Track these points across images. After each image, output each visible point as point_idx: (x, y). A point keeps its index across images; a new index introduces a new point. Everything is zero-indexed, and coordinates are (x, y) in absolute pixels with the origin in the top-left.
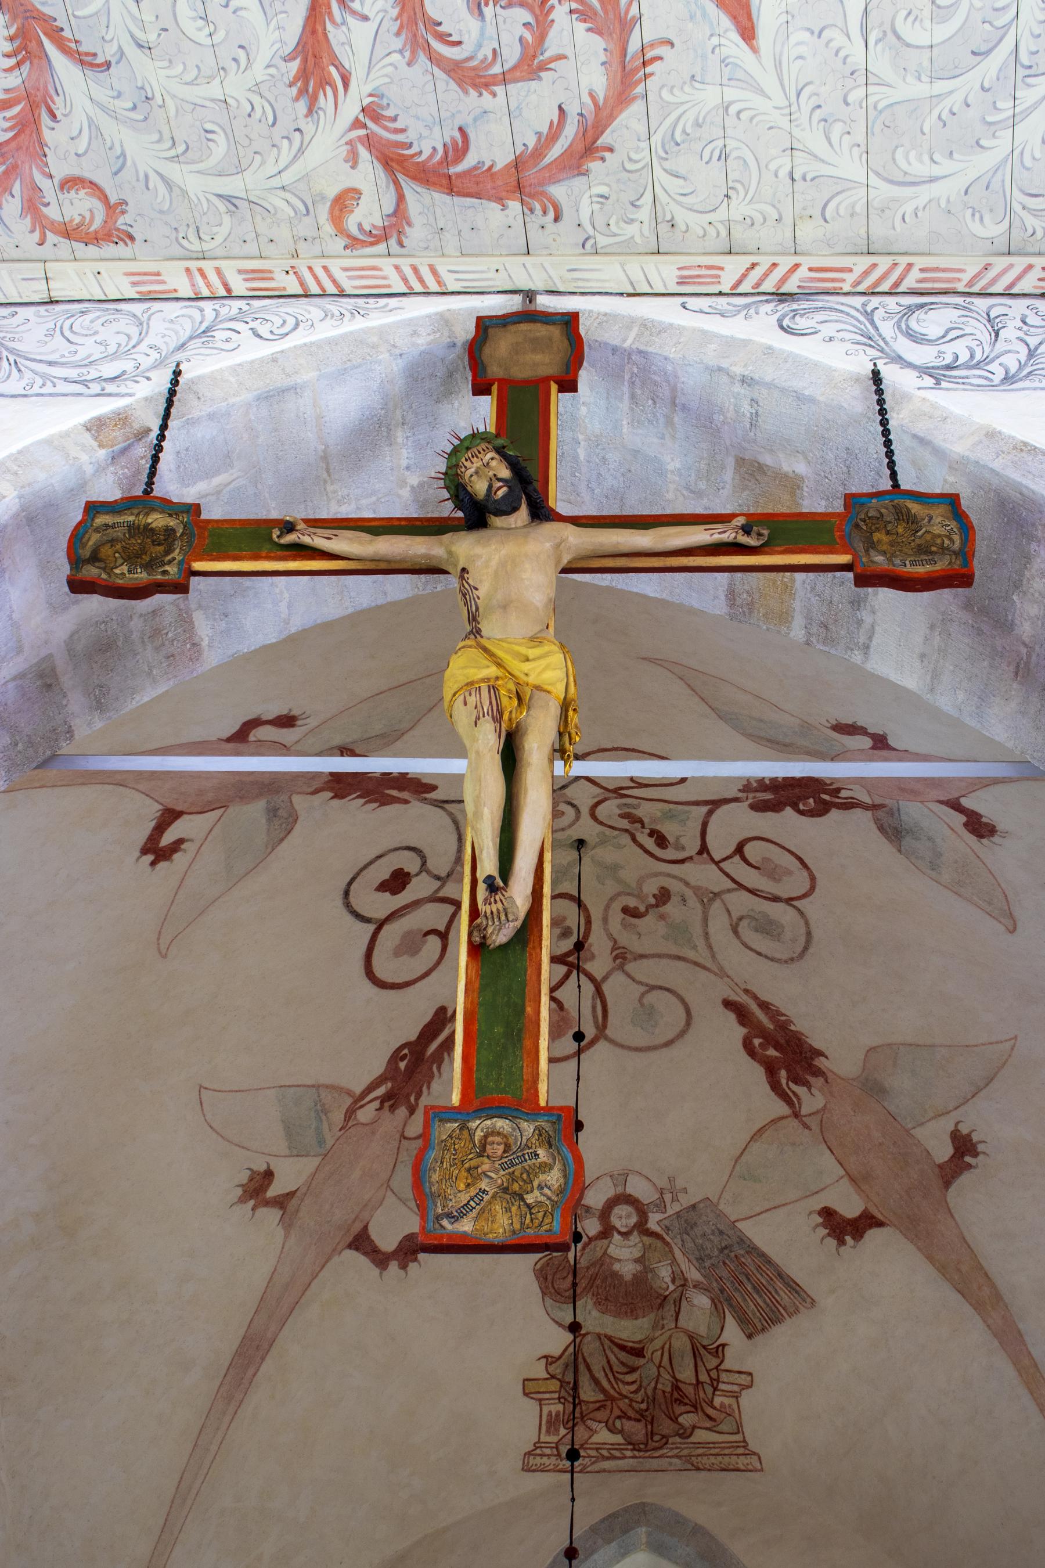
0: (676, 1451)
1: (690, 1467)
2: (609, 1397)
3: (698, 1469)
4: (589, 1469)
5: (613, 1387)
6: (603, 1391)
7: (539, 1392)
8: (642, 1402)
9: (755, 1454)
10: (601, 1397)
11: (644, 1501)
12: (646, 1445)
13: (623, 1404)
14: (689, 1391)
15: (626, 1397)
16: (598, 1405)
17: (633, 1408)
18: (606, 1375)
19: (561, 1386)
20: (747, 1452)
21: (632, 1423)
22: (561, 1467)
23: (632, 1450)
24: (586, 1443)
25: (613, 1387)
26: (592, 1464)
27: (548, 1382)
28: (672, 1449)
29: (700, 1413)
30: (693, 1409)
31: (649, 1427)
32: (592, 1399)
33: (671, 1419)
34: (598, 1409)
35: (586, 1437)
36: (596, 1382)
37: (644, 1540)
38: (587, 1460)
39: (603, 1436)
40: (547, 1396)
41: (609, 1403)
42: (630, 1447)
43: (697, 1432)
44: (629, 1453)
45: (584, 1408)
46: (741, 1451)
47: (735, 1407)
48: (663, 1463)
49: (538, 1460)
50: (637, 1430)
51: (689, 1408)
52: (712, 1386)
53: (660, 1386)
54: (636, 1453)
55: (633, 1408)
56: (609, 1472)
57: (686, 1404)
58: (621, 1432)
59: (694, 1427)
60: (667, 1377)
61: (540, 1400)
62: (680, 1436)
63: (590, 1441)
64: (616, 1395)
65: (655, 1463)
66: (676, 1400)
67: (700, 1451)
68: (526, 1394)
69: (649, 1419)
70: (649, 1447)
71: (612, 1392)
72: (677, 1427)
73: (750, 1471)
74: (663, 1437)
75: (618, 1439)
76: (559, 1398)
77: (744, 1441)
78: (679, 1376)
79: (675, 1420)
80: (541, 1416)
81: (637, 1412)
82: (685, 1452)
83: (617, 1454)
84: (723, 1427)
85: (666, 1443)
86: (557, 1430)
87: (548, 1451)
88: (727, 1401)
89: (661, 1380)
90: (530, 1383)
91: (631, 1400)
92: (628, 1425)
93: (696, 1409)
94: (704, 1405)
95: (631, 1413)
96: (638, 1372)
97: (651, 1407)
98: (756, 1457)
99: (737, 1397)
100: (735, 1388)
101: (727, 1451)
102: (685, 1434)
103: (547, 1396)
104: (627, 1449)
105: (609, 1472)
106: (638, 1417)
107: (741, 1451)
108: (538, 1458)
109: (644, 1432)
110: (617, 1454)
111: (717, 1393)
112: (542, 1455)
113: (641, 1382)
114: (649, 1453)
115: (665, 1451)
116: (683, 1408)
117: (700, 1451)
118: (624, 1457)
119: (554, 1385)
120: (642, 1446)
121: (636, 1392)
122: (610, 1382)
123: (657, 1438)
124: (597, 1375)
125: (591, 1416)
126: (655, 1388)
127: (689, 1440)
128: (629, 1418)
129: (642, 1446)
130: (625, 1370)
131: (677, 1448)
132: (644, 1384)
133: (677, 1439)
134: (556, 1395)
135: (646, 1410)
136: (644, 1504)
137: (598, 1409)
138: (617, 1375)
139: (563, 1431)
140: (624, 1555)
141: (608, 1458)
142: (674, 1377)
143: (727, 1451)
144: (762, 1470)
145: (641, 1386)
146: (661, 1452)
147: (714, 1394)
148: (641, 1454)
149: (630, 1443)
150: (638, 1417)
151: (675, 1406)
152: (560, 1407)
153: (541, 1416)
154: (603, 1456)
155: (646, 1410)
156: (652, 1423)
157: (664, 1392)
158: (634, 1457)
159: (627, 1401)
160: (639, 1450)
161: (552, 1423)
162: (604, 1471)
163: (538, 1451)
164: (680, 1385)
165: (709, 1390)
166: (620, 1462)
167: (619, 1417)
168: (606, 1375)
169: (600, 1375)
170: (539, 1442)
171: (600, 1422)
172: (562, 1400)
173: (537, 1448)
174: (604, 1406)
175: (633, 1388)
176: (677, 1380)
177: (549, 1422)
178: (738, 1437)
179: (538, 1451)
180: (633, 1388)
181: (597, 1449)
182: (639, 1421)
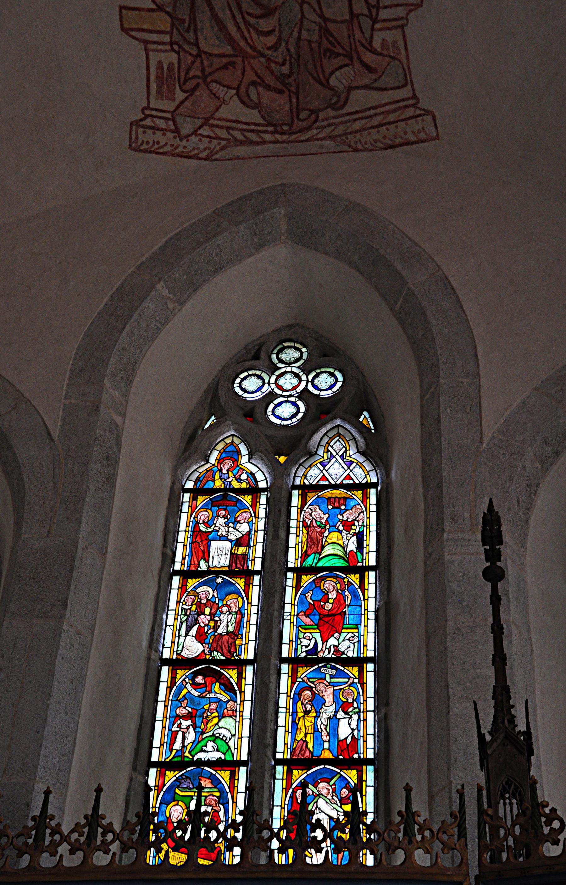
0: (328, 130)
1: (346, 148)
2: (238, 51)
3: (356, 150)
4: (217, 156)
5: (243, 37)
6: (231, 41)
7: (143, 30)
8: (283, 64)
9: (428, 112)
10: (229, 50)
11: (285, 182)
12: (291, 125)
13: (259, 63)
14: (340, 32)
15: (263, 55)
16: (225, 60)
17: (272, 72)
18: (234, 16)
19: (173, 25)
20: (418, 112)
21: (273, 94)
22: (180, 149)
23: (273, 133)
24: (212, 117)
25: (243, 37)
26: (221, 149)
27: (154, 15)
28: (324, 127)
29: (357, 63)
30: (347, 61)
31: (294, 100)
32: (216, 51)
33: (321, 83)
34: (225, 67)
35: (212, 108)
36: (222, 27)
37: (284, 228)
38: (215, 142)
39: (233, 110)
40: (154, 37)
41: (239, 60)
42: (270, 129)
43: (355, 95)
44: (268, 137)
45: (206, 63)
46: (410, 112)
47: (401, 44)
48: (313, 146)
49: (150, 136)
50: (279, 104)
51: (342, 60)
52: (370, 17)
53: (305, 34)
54: (279, 137)
55: (272, 72)
56: (244, 159)
57: (339, 55)
58: (257, 106)
59: (350, 89)
60: (313, 17)
61: (146, 42)
62: (333, 107)
63: (217, 115)
64: (249, 50)
65: (302, 148)
66: (327, 50)
67: (358, 125)
68: (125, 30)
69: (293, 89)
70: (294, 129)
71: (242, 43)
72: (329, 93)
73: (423, 141)
74: (312, 111)
75: (254, 116)
76: (171, 43)
77: (415, 97)
78: (328, 13)
79: (326, 85)
80: (148, 68)
81: (277, 78)
82: (340, 130)
83: (254, 137)
84: (387, 80)
85: (316, 121)
86: (172, 92)
87: (161, 124)
88: (389, 36)
89: (305, 23)
90: (130, 13)
91: (269, 60)
92: (267, 97)
93: (351, 59)
94: (361, 49)
95: (270, 80)
96: (276, 16)
97: (295, 70)
98: (429, 118)
99: (402, 27)
100: (400, 12)
101: (391, 118)
102: (338, 102)
103: (154, 37)
104: (266, 132)
105: (244, 159)
106: (279, 86)
107: (410, 112)
108: (149, 132)
109: (287, 108)
110: (254, 137)
111: (377, 26)
112: (155, 129)
113: (281, 32)
114: (293, 137)
115: (315, 131)
116: (336, 62)
117: (358, 125)
118: (264, 142)
119: (163, 22)
120: (285, 128)
121: (274, 47)
122: (239, 28)
123: (304, 115)
124: (221, 15)
125: (217, 76)
126: (299, 39)
127: (344, 111)
128: (268, 87)
129: (285, 128)
130: (258, 12)
131: (329, 125)
132: (285, 35)
133: (330, 112)
134: (167, 38)
135: (289, 76)
136: (284, 185)
137: (225, 67)
138: (248, 18)
139: (180, 96)
140: (259, 247)
141: (242, 143)
142: (322, 16)
143: (391, 118)
144: (437, 138)
145: (280, 39)
146: (309, 134)
147: (373, 29)
148: (285, 137)
149: (270, 124)
150: (279, 86)
151: (325, 61)
152: (173, 58)
153: (148, 68)
154: (236, 140)
155: (289, 76)
156: (297, 94)
157: (310, 42)
158: (276, 142)
159: (263, 60)
160: (282, 133)
161: (164, 81)
162: (238, 158)
163: (148, 122)
164: (330, 26)
165: (366, 23)
166: (259, 148)
167: (253, 83)
168: (234, 16)
169: (225, 16)
170: (148, 108)
171: (229, 87)
172: (176, 47)
173: (147, 116)
174: (233, 64)
175: (271, 40)
176: (326, 20)
177: (159, 77)
178: (406, 92)
179: (148, 122)
180: (271, 40)
181: (228, 129)
182: (280, 92)
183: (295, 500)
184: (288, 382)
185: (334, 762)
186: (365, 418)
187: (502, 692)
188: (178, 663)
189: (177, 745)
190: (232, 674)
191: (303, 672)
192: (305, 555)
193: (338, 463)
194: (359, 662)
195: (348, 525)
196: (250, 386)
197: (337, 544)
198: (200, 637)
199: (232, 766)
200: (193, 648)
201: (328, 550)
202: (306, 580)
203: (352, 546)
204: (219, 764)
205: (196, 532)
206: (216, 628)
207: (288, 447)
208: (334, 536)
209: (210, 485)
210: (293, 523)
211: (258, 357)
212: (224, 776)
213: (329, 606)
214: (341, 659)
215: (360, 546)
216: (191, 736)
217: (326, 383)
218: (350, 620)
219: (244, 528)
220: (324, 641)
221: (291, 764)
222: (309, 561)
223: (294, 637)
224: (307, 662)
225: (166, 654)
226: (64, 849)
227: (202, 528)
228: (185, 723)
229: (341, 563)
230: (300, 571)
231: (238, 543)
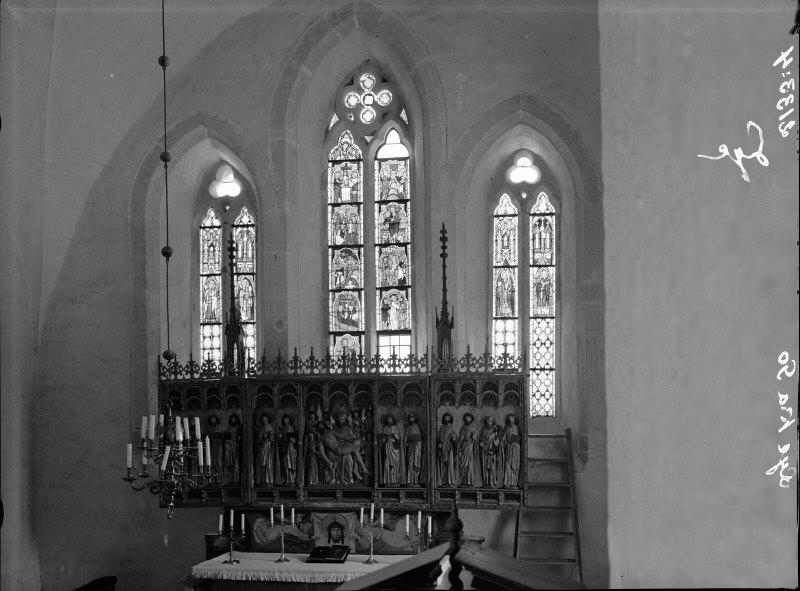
183: (376, 167)
184: (369, 100)
185: (396, 288)
186: (403, 115)
187: (445, 303)
188: (335, 247)
189: (338, 283)
190: (355, 251)
191: (384, 250)
192: (381, 195)
193: (393, 146)
194: (405, 245)
195: (399, 179)
196: (352, 100)
197: (396, 189)
198: (342, 235)
199: (359, 290)
200: (340, 241)
201: (391, 192)
202: (383, 207)
203: (401, 190)
204: (354, 290)
205: (335, 183)
206: (347, 231)
207: (368, 136)
208: (393, 185)
209: (338, 158)
210: (376, 178)
211: (352, 83)
212: (356, 294)
213: (393, 220)
214: (399, 244)
215: (404, 190)
216: (343, 279)
217: (385, 98)
218: (401, 226)
219: (355, 181)
220: (392, 236)
221: (382, 289)
222: (384, 198)
223: (379, 236)
224: (387, 245)
225: (330, 244)
226: (304, 368)
227: (338, 181)
228: (340, 273)
229: (396, 198)
230: (381, 203)
231: (353, 189)
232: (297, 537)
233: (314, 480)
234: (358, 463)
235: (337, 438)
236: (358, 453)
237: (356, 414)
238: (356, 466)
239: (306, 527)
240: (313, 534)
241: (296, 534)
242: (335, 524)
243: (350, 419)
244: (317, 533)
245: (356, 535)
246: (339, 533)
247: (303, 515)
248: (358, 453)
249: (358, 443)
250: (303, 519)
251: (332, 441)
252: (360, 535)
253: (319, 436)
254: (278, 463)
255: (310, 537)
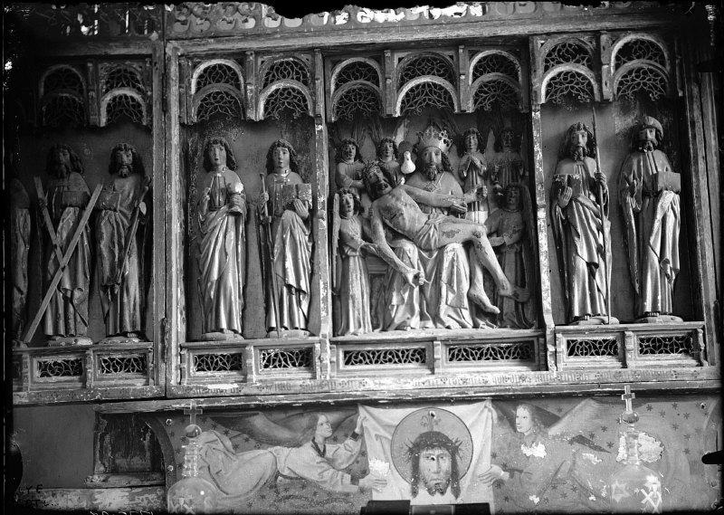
232: (315, 484)
233: (361, 329)
234: (488, 273)
235: (423, 205)
236: (487, 245)
237: (474, 141)
238: (479, 275)
239: (344, 451)
240: (365, 472)
241: (312, 475)
242: (432, 440)
243: (453, 160)
244: (378, 465)
245: (497, 469)
246: (446, 464)
247: (334, 417)
248: (487, 245)
249: (481, 215)
250: (336, 427)
251: (411, 215)
252: (505, 467)
253: (366, 203)
254: (257, 280)
255: (354, 480)
